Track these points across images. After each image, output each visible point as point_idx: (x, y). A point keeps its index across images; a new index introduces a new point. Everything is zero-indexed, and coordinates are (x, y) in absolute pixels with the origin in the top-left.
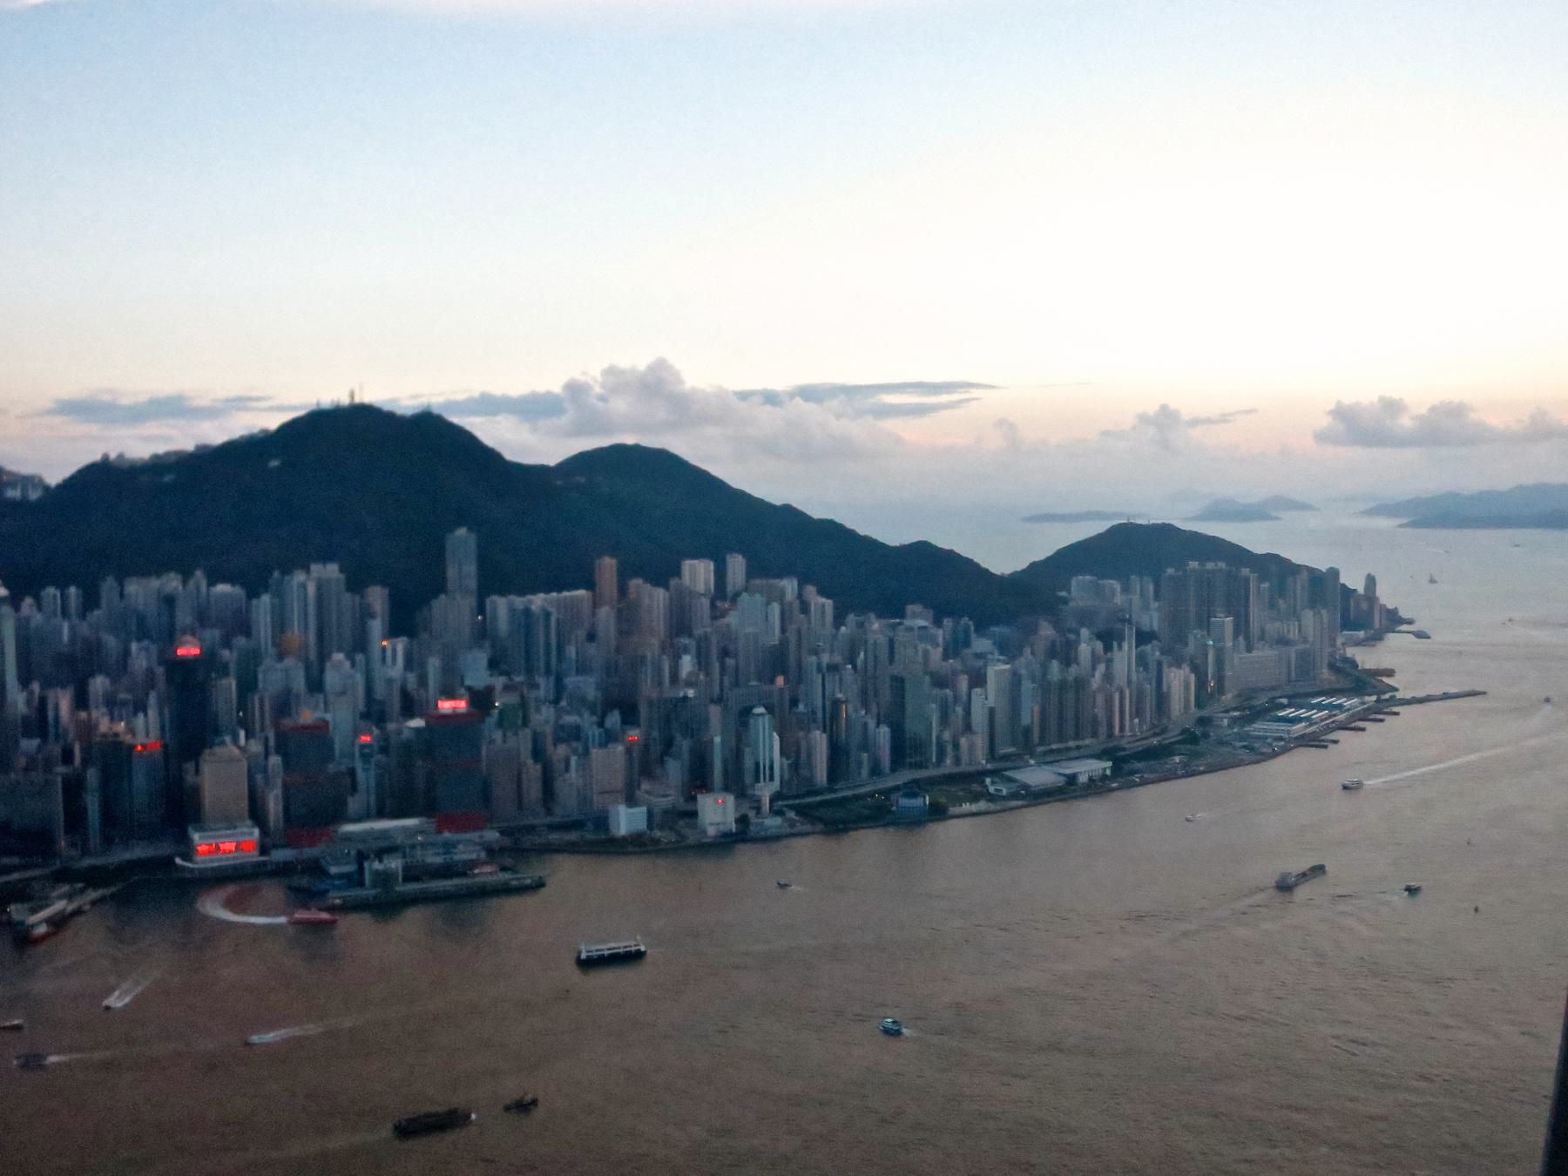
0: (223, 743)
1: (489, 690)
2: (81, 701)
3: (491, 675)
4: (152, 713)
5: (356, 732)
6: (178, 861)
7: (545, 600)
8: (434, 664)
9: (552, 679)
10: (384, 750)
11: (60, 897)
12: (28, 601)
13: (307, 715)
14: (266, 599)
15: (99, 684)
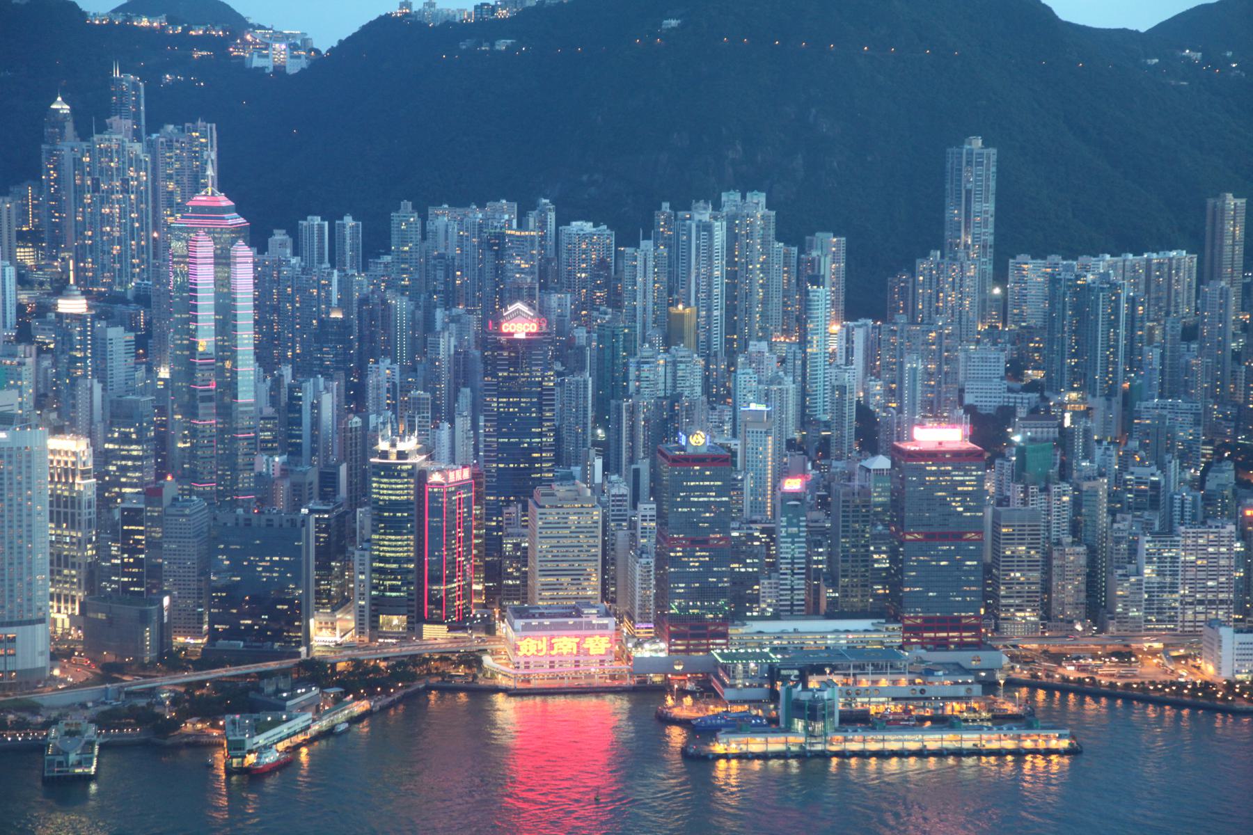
0: (569, 477)
1: (1005, 415)
2: (355, 398)
3: (1010, 390)
4: (463, 423)
5: (783, 472)
6: (487, 660)
7: (1113, 266)
8: (914, 363)
9: (1118, 399)
10: (824, 503)
11: (303, 709)
12: (279, 236)
13: (699, 440)
14: (646, 245)
15: (383, 372)
